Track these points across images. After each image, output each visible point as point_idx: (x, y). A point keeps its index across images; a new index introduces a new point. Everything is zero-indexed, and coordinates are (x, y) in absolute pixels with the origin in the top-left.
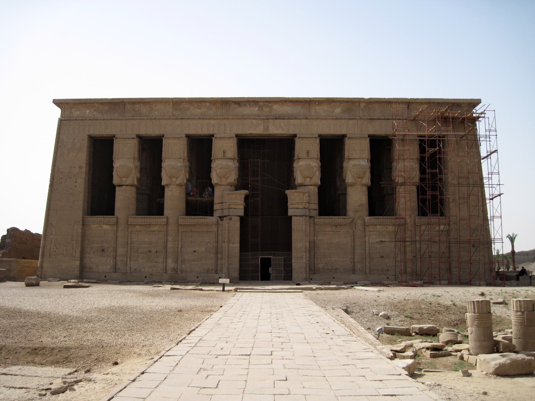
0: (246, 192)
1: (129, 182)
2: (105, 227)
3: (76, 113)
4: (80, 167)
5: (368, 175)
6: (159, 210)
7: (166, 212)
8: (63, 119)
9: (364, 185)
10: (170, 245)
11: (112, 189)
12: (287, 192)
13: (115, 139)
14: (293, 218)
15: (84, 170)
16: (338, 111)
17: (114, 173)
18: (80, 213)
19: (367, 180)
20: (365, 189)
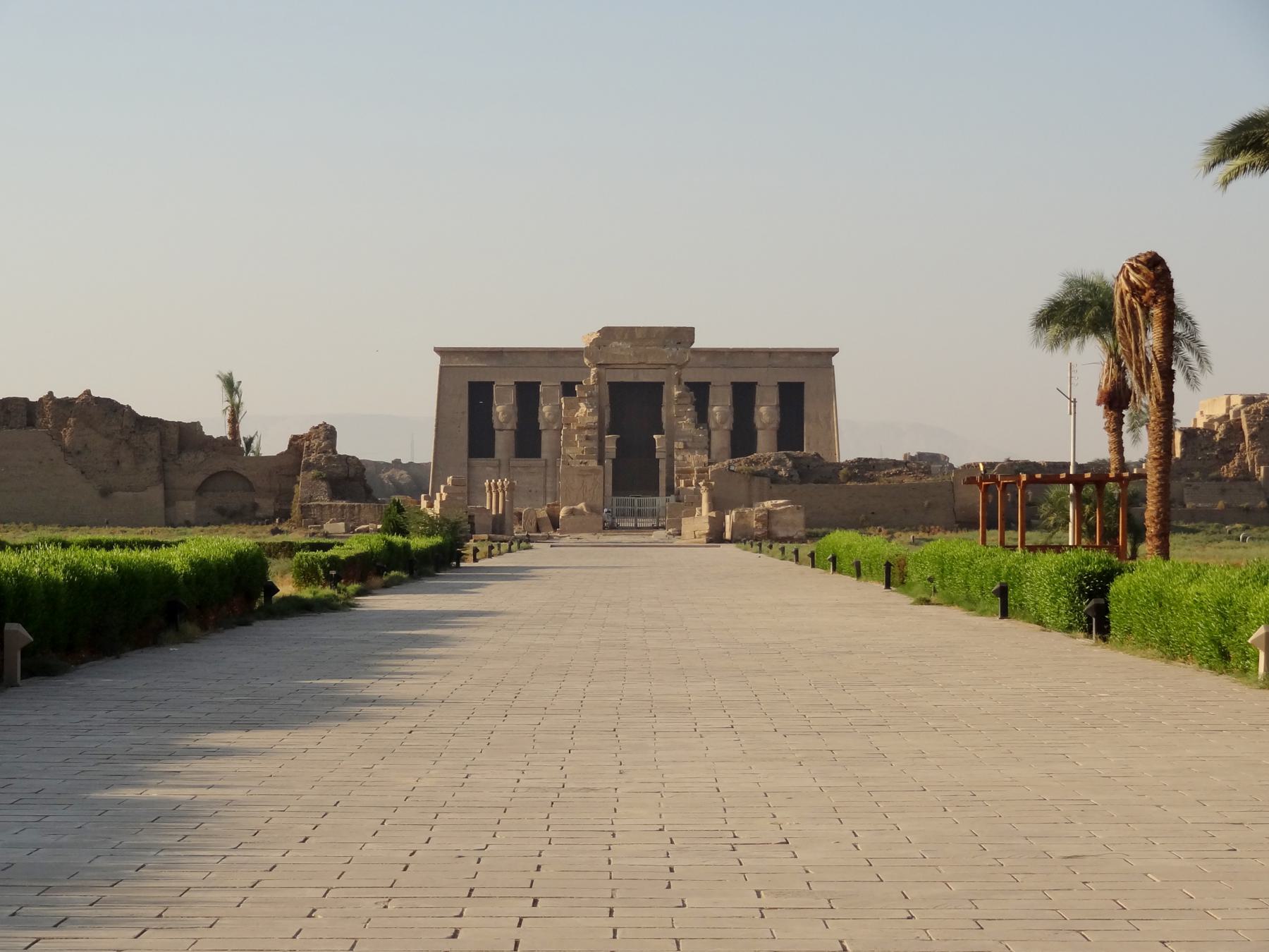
0: (618, 436)
1: (509, 428)
2: (488, 468)
3: (456, 362)
4: (463, 413)
5: (731, 420)
6: (537, 454)
7: (544, 455)
8: (444, 365)
9: (726, 430)
10: (549, 485)
11: (491, 433)
12: (655, 436)
13: (494, 386)
14: (660, 460)
15: (466, 415)
16: (703, 359)
17: (494, 418)
18: (466, 455)
19: (728, 426)
20: (728, 434)
